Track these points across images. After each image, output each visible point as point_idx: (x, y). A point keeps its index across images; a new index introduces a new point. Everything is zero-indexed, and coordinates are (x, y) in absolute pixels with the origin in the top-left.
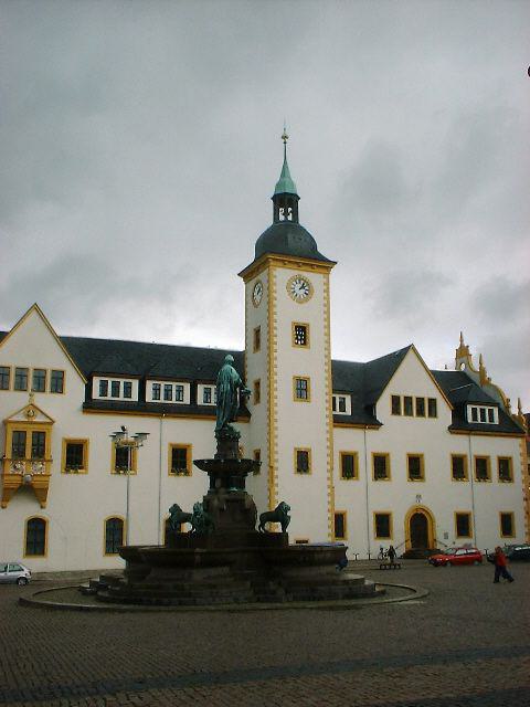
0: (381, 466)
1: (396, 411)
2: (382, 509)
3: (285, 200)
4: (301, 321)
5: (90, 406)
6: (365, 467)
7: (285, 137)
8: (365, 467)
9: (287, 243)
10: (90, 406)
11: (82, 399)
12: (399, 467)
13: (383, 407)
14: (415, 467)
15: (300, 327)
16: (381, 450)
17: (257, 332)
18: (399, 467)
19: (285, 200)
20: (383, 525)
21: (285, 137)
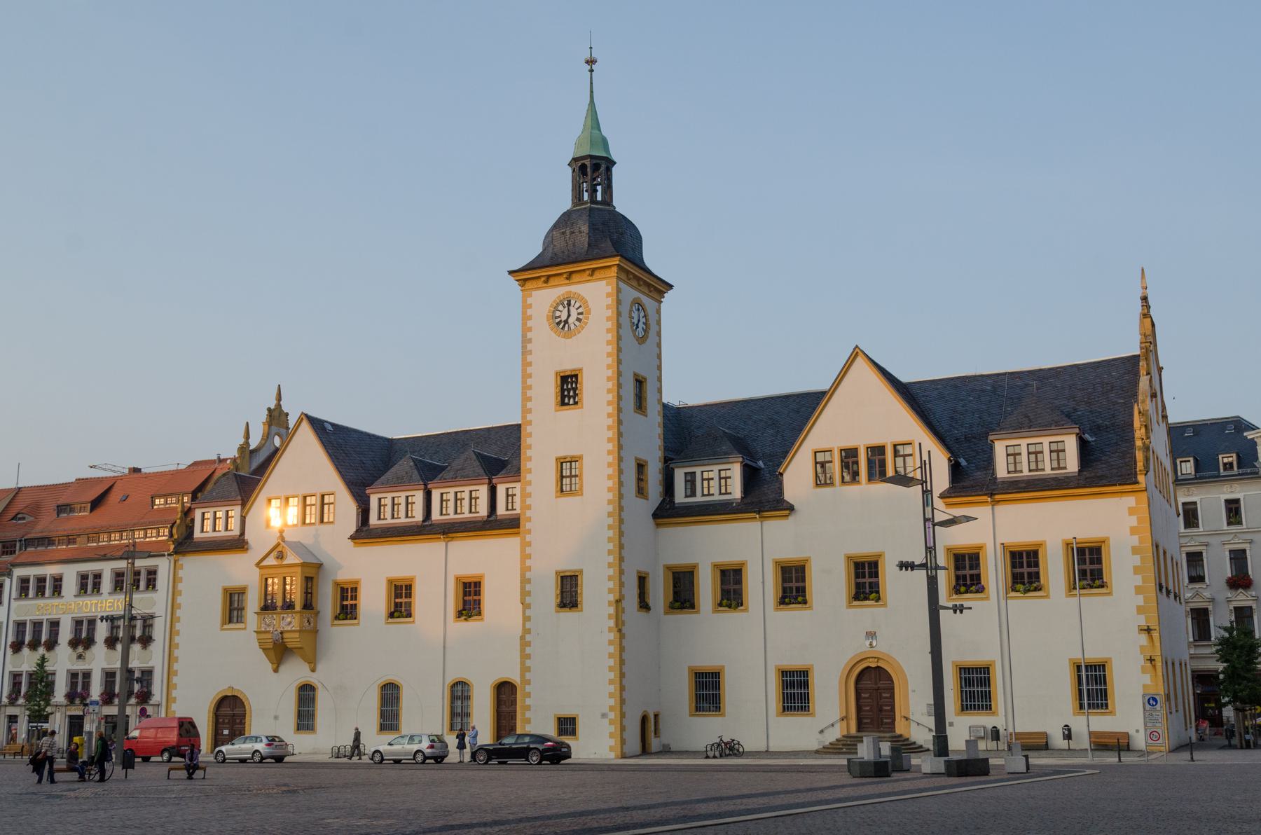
0: (793, 585)
1: (822, 479)
2: (794, 662)
3: (593, 169)
4: (568, 367)
5: (365, 532)
6: (761, 586)
7: (591, 62)
8: (761, 586)
9: (596, 234)
10: (365, 532)
11: (352, 528)
12: (828, 582)
13: (797, 478)
14: (865, 579)
15: (571, 376)
16: (790, 554)
17: (640, 382)
18: (828, 582)
19: (593, 169)
20: (795, 690)
21: (591, 62)
